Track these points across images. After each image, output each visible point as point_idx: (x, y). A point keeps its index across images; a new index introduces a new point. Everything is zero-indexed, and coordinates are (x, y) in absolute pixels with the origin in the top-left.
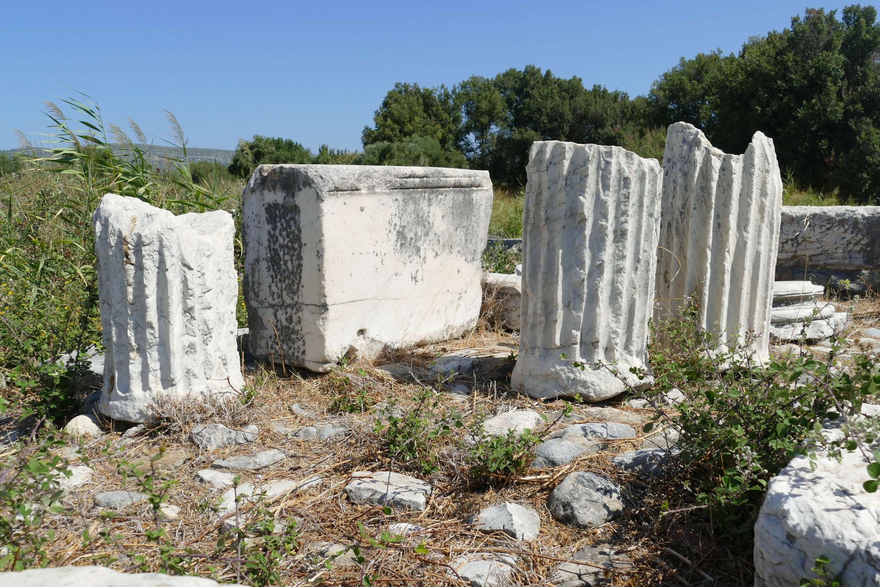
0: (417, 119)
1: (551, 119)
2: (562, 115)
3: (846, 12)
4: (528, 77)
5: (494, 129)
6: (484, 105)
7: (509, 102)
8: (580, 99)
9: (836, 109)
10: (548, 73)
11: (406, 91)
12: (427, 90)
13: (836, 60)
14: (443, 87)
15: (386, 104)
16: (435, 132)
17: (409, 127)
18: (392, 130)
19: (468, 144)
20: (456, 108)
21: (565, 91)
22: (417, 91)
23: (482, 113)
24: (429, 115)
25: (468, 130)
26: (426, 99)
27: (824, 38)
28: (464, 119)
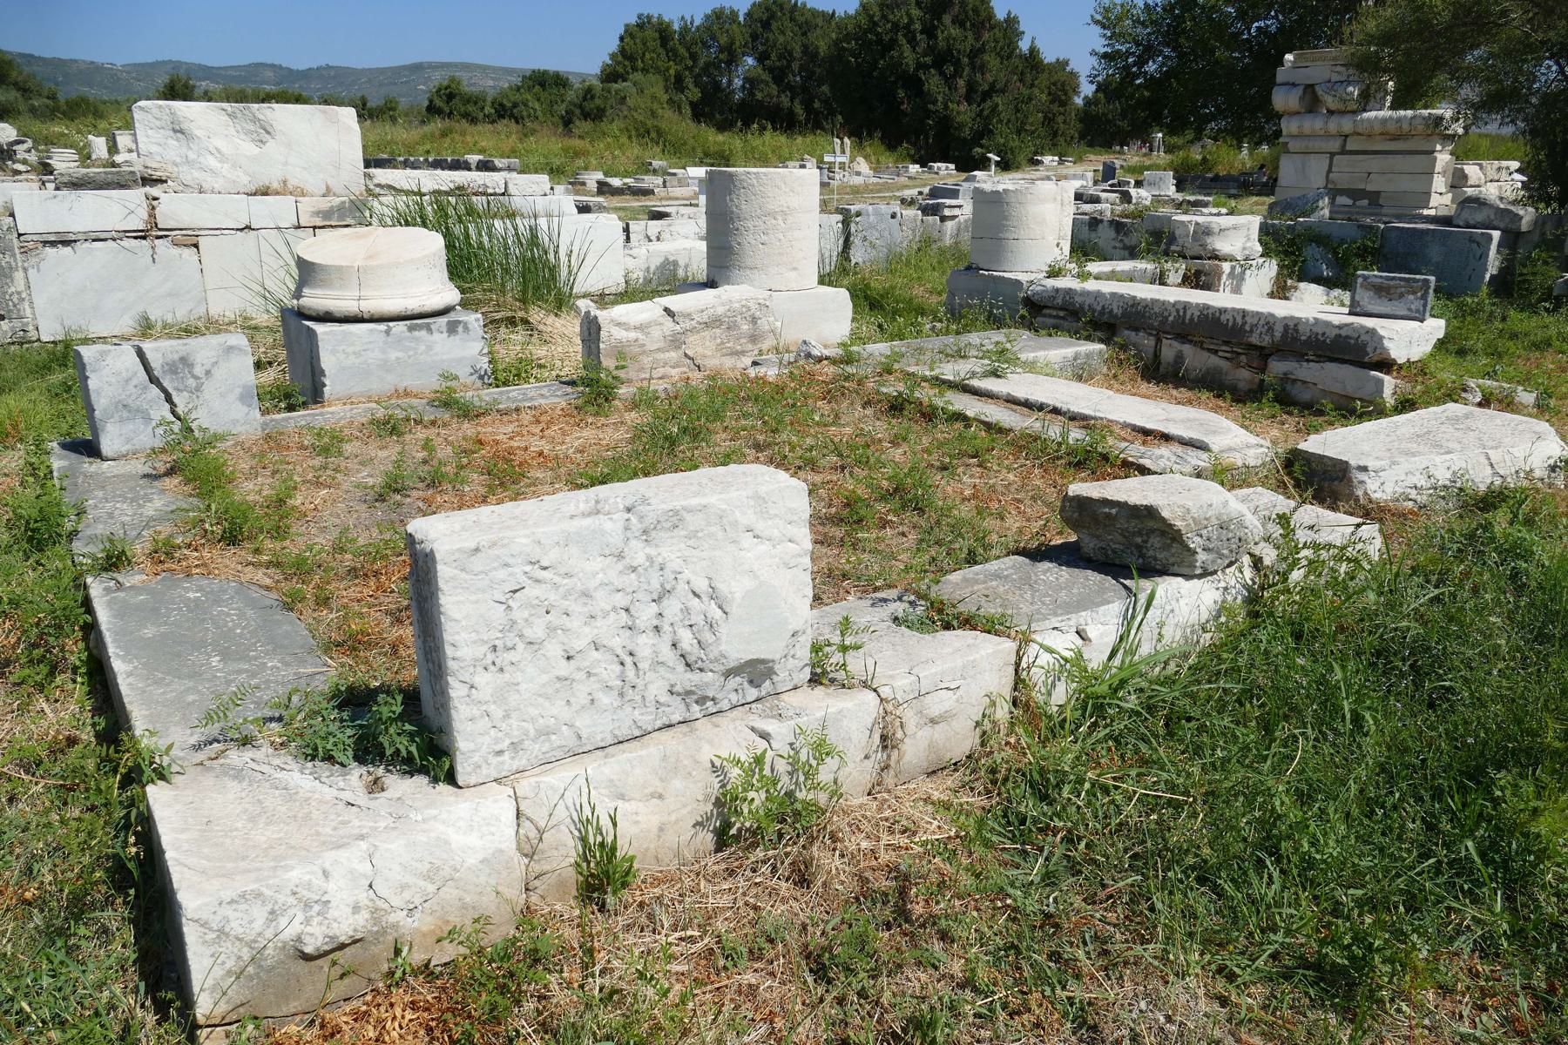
1: (780, 57)
2: (790, 54)
11: (649, 22)
16: (668, 69)
26: (663, 32)
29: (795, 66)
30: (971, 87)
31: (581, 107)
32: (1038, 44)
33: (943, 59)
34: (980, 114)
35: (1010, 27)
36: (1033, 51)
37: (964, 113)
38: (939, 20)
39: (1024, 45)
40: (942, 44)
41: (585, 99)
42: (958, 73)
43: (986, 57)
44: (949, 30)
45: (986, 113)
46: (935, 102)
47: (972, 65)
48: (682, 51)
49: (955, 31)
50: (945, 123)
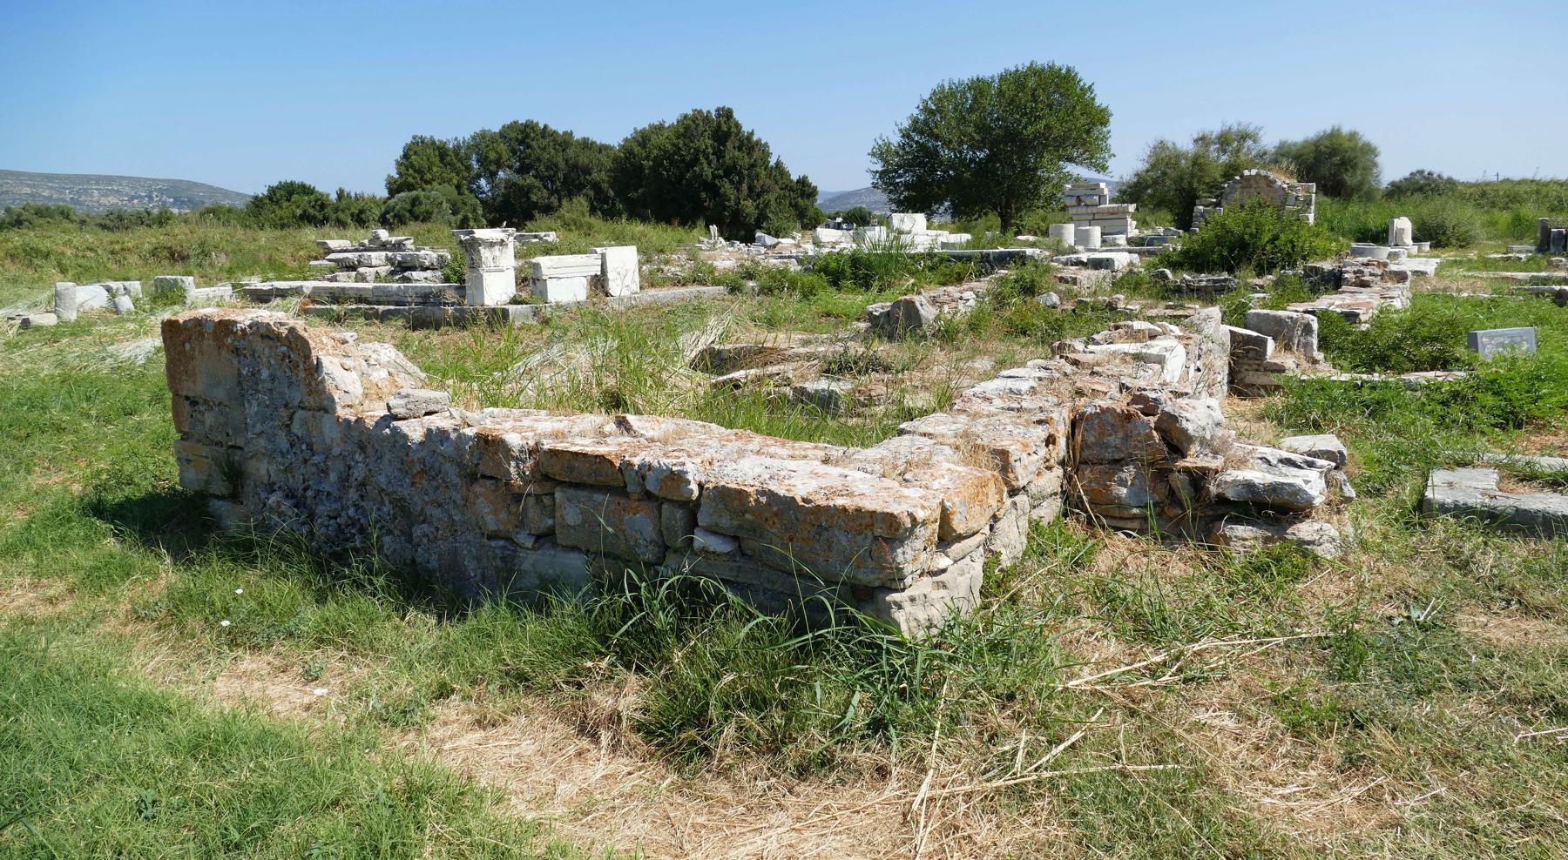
0: (435, 169)
1: (548, 168)
2: (556, 165)
3: (718, 110)
4: (528, 130)
6: (492, 156)
7: (514, 152)
8: (570, 152)
9: (708, 172)
10: (545, 127)
11: (422, 142)
12: (441, 142)
13: (706, 143)
14: (456, 139)
15: (406, 156)
16: (451, 179)
17: (428, 176)
18: (414, 178)
19: (479, 187)
20: (469, 158)
21: (560, 145)
22: (434, 143)
23: (491, 162)
24: (446, 166)
25: (479, 176)
26: (441, 151)
27: (701, 129)
28: (475, 166)
29: (560, 175)
30: (751, 189)
31: (410, 212)
32: (782, 159)
33: (730, 171)
34: (757, 207)
36: (778, 164)
37: (749, 206)
38: (725, 146)
39: (772, 161)
42: (740, 182)
44: (731, 152)
45: (761, 206)
46: (729, 200)
47: (749, 176)
48: (459, 165)
49: (737, 153)
50: (737, 214)
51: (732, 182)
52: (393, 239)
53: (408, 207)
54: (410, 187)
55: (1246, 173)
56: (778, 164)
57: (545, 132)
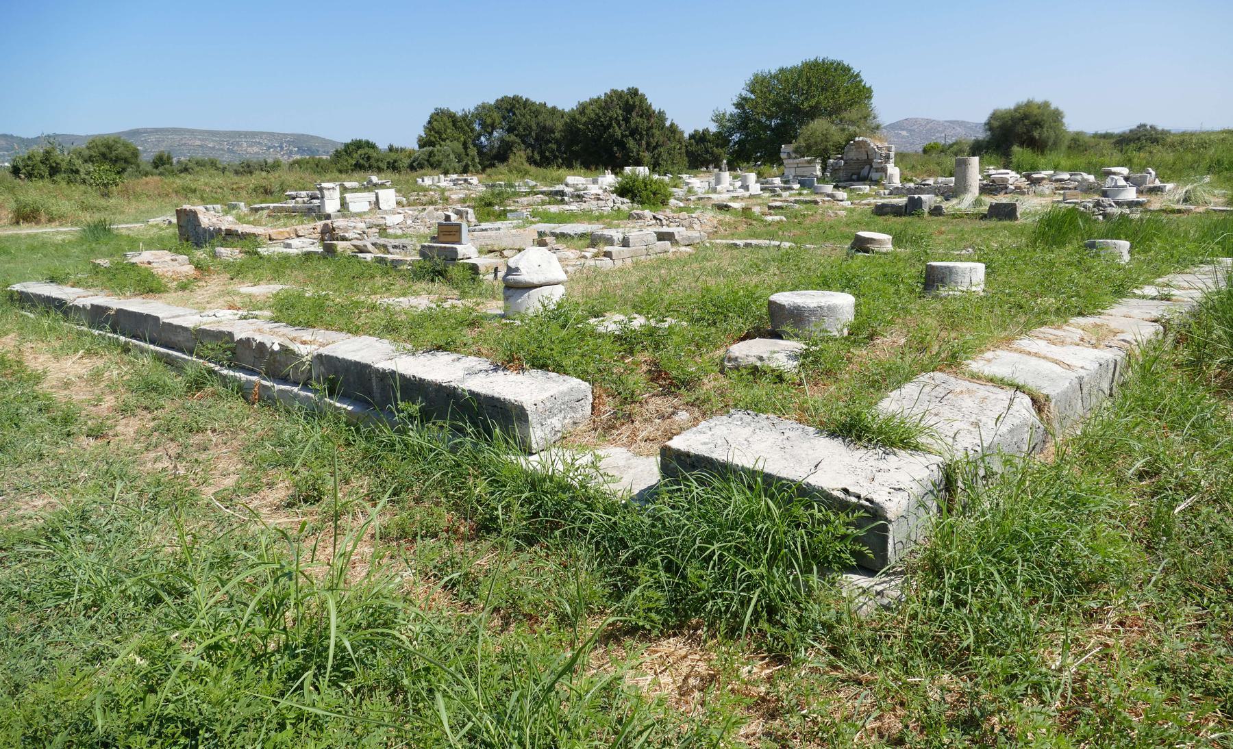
0: (449, 131)
2: (530, 127)
5: (495, 134)
6: (489, 121)
7: (504, 118)
8: (541, 118)
9: (618, 133)
15: (430, 122)
17: (444, 136)
20: (471, 122)
25: (480, 135)
26: (453, 118)
28: (477, 127)
29: (533, 134)
30: (648, 144)
31: (428, 161)
32: (675, 122)
33: (634, 132)
34: (653, 157)
35: (661, 116)
36: (672, 125)
39: (668, 124)
40: (633, 126)
41: (430, 156)
42: (641, 139)
43: (654, 131)
44: (635, 119)
47: (647, 134)
49: (639, 119)
51: (635, 139)
52: (380, 182)
53: (426, 158)
54: (432, 144)
55: (857, 139)
56: (672, 125)
57: (526, 104)
